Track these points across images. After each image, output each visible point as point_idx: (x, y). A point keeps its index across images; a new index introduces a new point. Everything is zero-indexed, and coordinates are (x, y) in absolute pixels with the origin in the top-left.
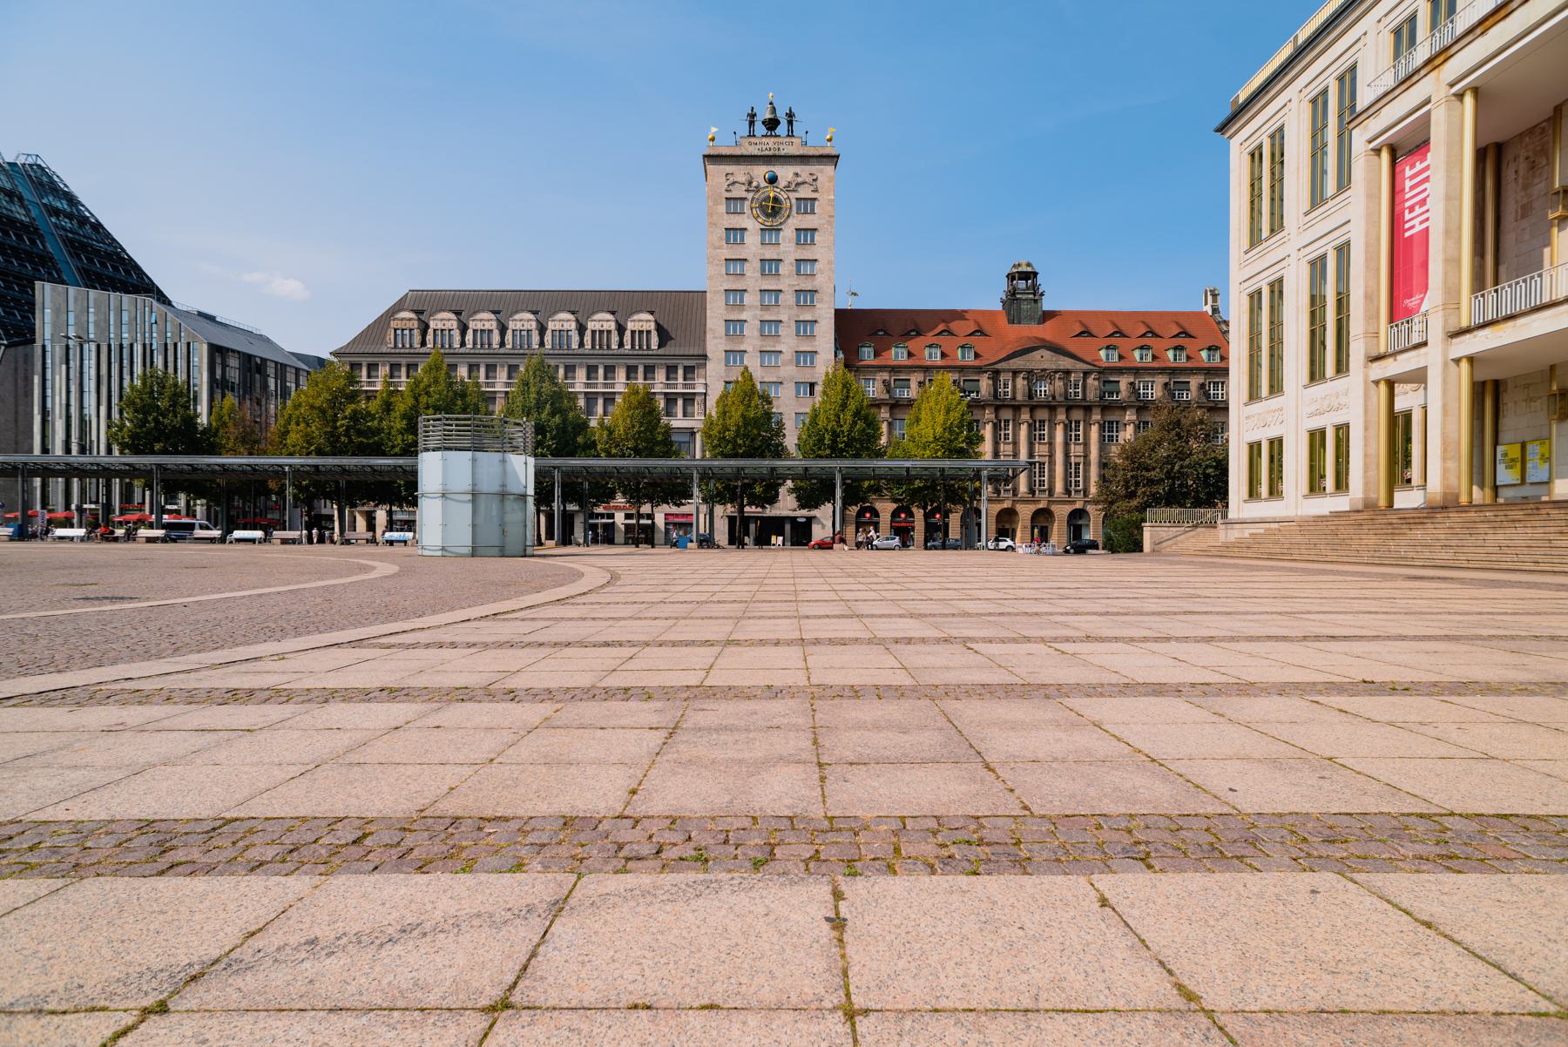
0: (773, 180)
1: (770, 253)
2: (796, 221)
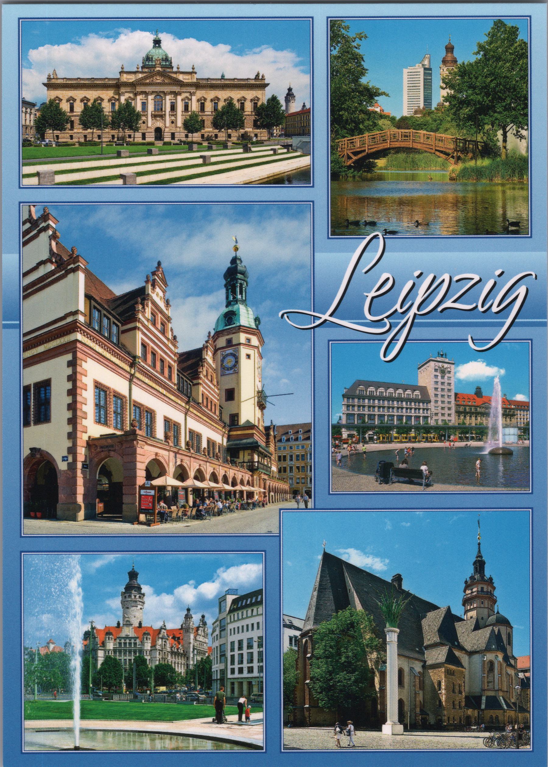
0: (443, 367)
1: (443, 381)
2: (447, 375)
